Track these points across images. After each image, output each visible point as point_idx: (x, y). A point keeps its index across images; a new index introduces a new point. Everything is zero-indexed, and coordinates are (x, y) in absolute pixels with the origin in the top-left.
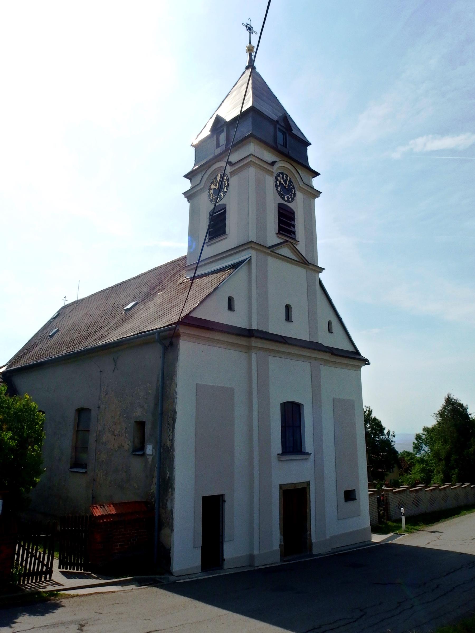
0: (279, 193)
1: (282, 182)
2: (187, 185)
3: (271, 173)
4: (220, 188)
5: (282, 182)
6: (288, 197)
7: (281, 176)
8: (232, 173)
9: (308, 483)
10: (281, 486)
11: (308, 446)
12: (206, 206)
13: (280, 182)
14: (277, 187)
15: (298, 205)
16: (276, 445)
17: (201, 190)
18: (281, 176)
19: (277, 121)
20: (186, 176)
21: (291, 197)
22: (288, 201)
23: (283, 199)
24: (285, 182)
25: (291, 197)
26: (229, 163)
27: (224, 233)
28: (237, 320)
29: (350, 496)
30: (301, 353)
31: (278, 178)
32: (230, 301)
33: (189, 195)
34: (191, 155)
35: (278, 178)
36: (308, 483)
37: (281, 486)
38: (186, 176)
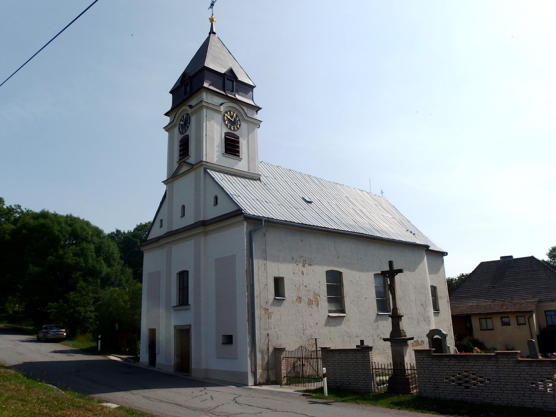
0: (227, 125)
1: (229, 117)
2: (167, 120)
3: (219, 112)
4: (185, 124)
5: (229, 117)
6: (234, 128)
7: (229, 113)
8: (193, 113)
9: (190, 326)
10: (175, 327)
11: (191, 300)
12: (177, 137)
13: (227, 117)
14: (224, 121)
15: (242, 133)
16: (174, 301)
17: (175, 125)
18: (229, 113)
19: (225, 74)
20: (166, 114)
21: (237, 127)
22: (234, 130)
23: (230, 129)
24: (232, 117)
25: (237, 127)
26: (191, 107)
27: (188, 155)
28: (189, 220)
29: (229, 340)
30: (169, 240)
31: (226, 115)
32: (216, 203)
33: (167, 128)
34: (169, 98)
35: (226, 115)
36: (190, 326)
37: (175, 327)
38: (166, 114)
